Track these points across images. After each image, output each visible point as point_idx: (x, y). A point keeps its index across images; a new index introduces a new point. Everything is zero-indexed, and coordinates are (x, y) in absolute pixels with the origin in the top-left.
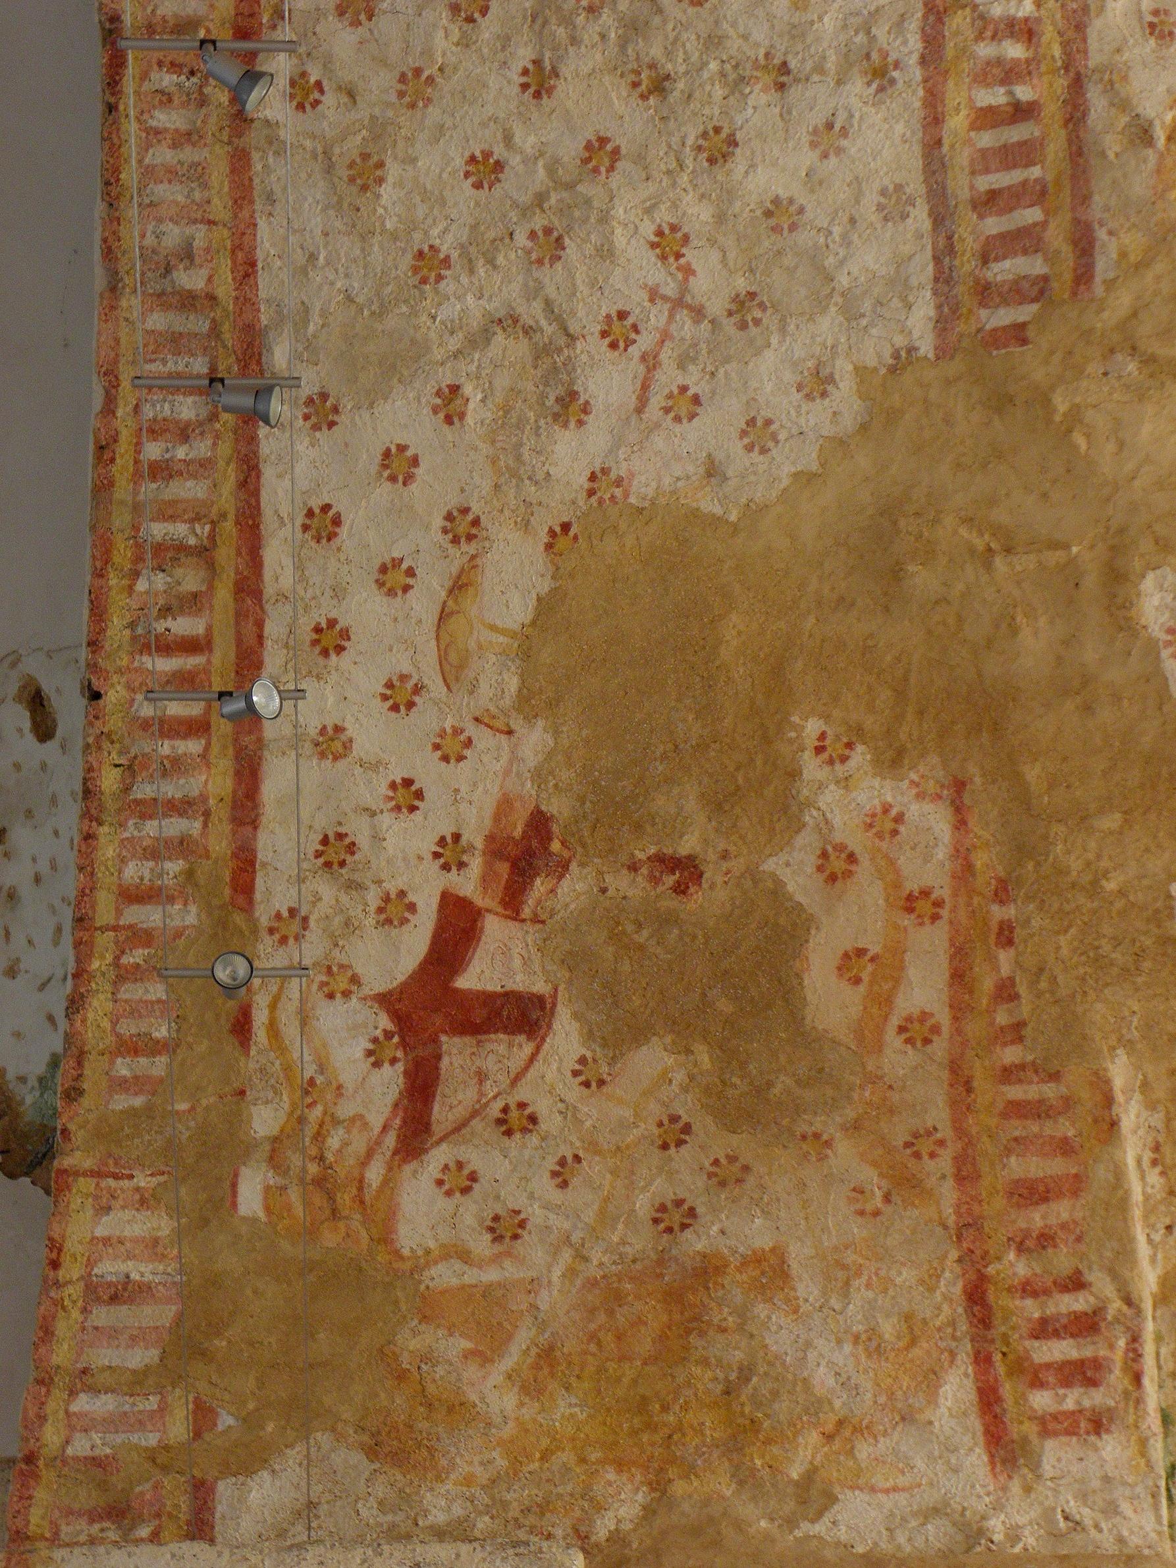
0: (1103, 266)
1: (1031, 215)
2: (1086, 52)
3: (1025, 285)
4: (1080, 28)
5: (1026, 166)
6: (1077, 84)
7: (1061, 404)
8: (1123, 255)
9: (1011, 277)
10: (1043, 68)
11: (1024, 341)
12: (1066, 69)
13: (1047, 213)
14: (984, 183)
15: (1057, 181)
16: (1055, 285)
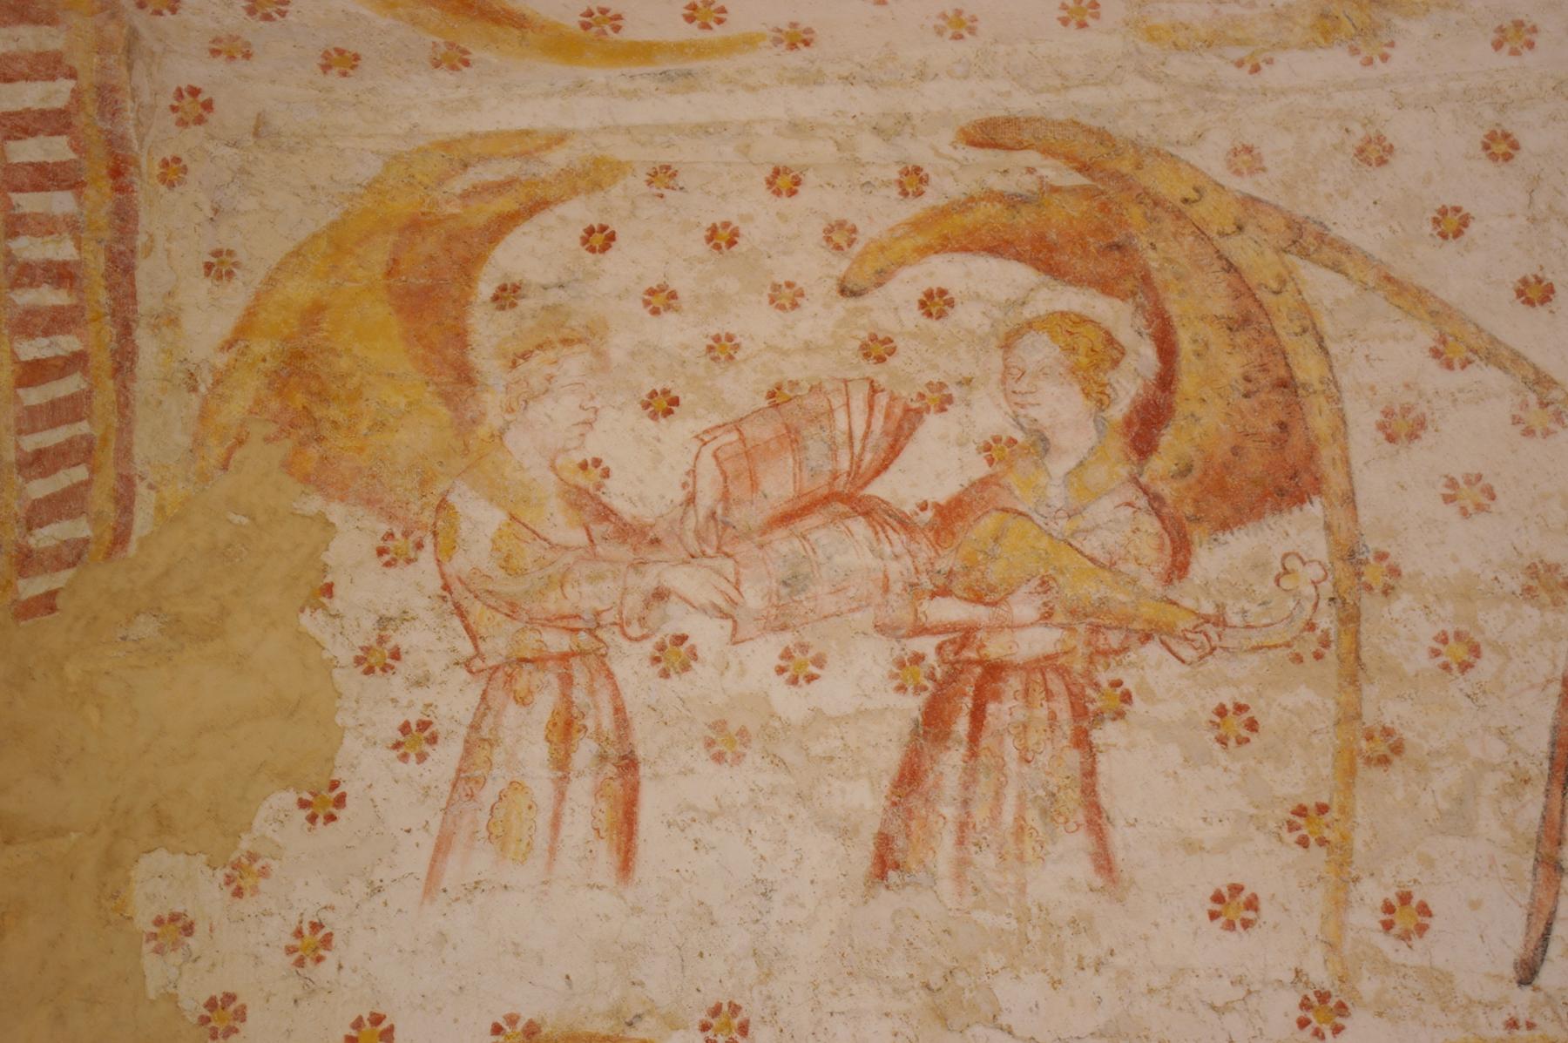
0: (143, 521)
1: (80, 473)
2: (133, 296)
3: (65, 551)
4: (129, 270)
5: (73, 421)
6: (126, 330)
7: (73, 671)
8: (160, 509)
9: (54, 542)
10: (88, 315)
11: (52, 609)
12: (113, 316)
13: (92, 471)
14: (30, 443)
15: (104, 439)
16: (92, 547)
